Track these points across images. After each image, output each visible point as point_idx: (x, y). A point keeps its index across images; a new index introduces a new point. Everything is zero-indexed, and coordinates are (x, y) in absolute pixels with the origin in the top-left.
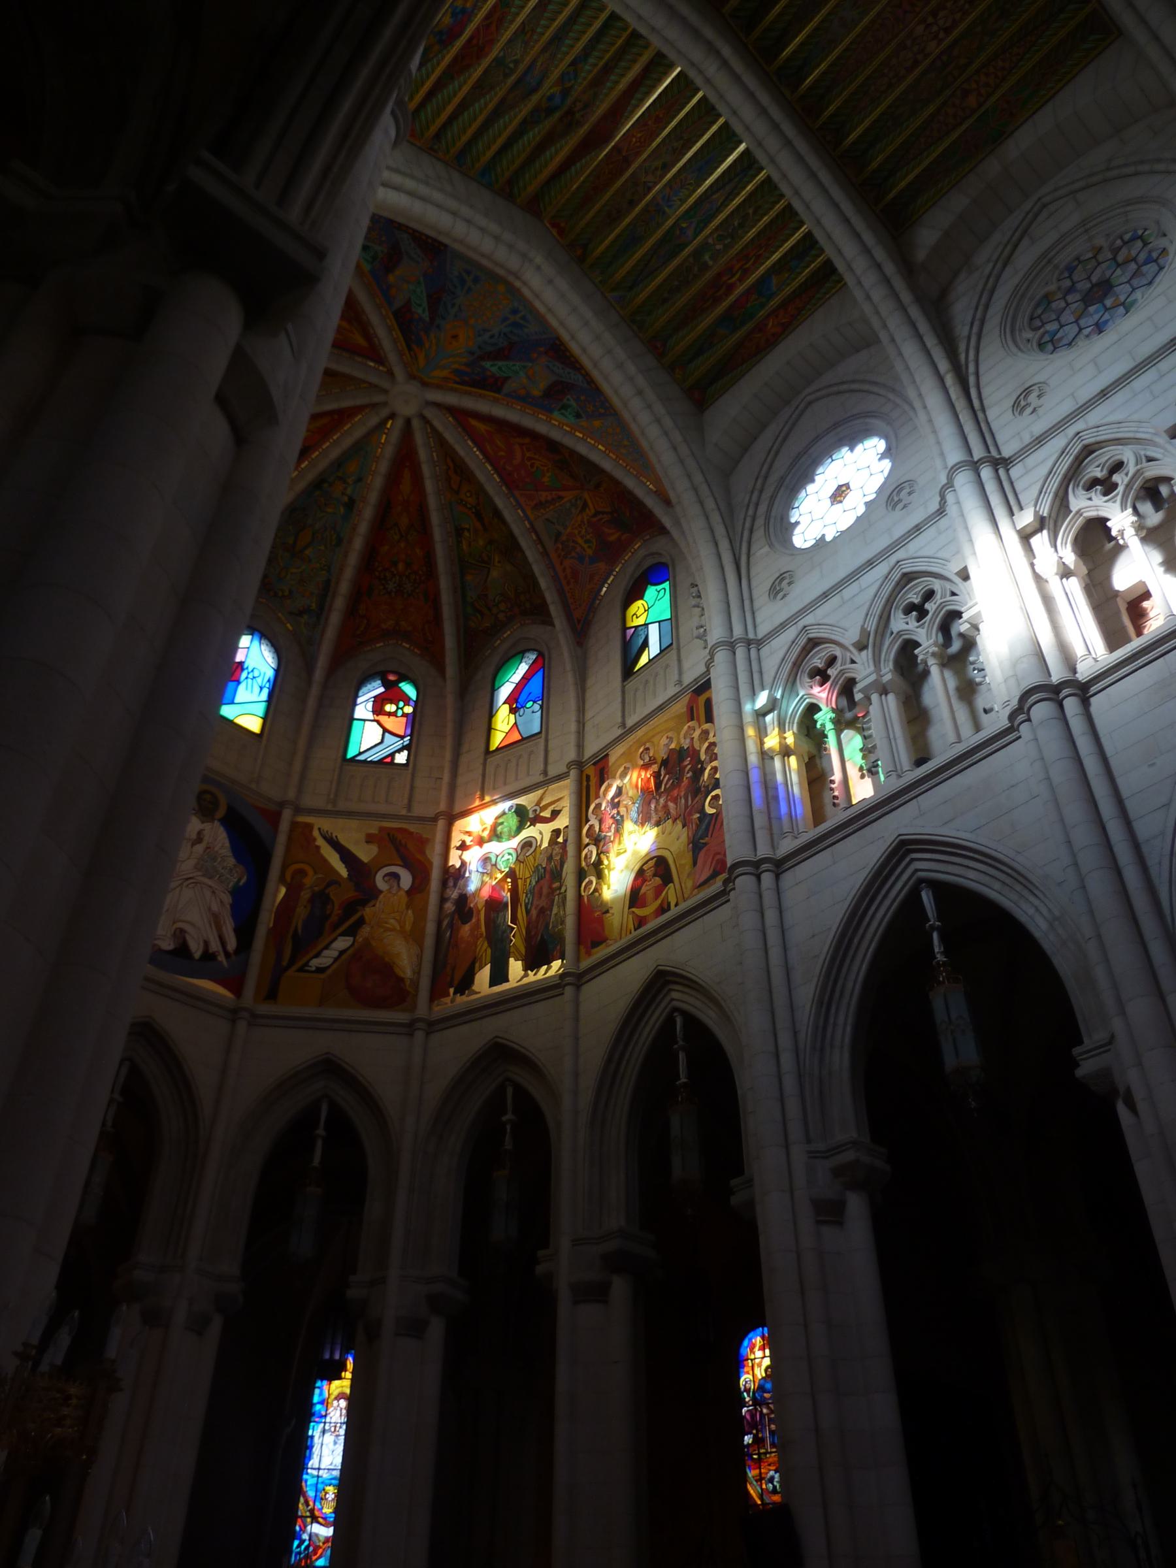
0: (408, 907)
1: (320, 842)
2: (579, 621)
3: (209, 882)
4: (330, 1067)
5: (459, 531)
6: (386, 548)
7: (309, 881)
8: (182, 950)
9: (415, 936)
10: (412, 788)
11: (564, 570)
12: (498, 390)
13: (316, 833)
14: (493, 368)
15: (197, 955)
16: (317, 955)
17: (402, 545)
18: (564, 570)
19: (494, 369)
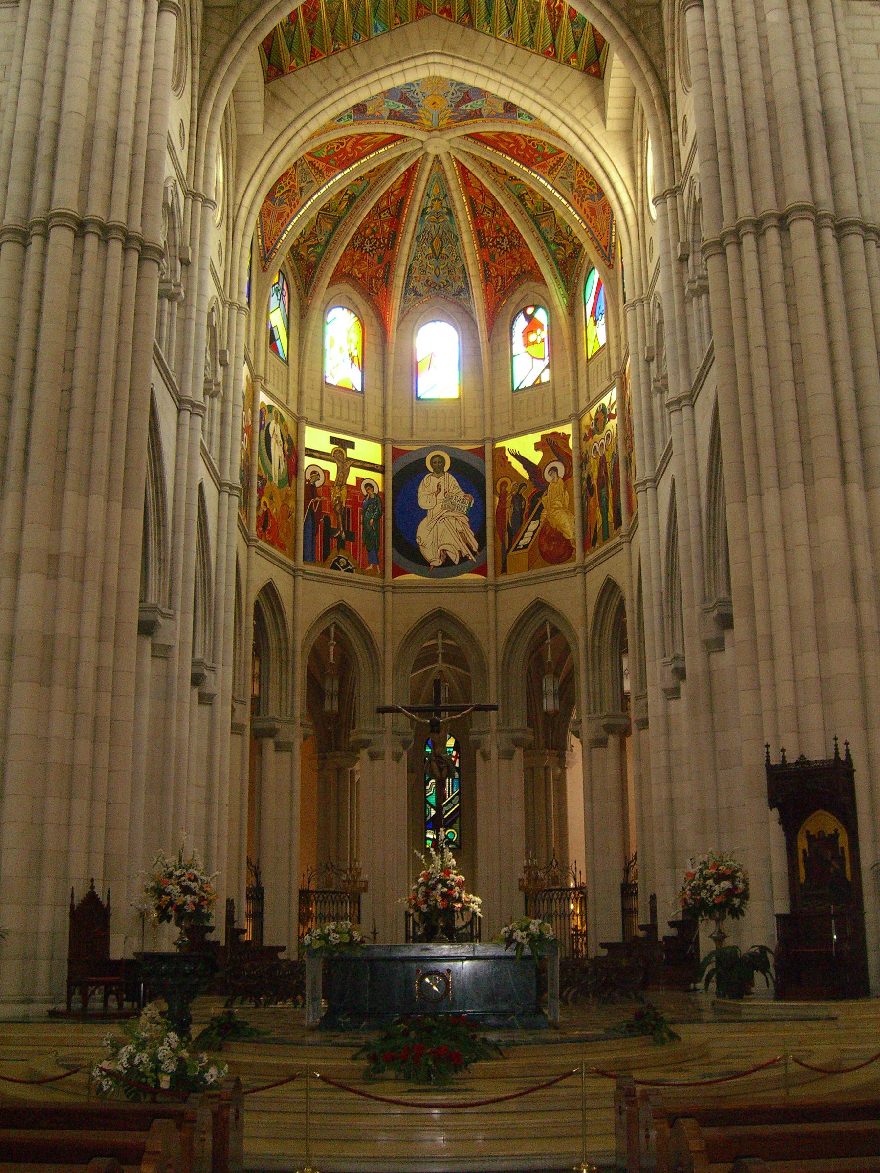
0: (565, 489)
1: (511, 459)
2: (606, 248)
3: (450, 514)
4: (539, 606)
5: (521, 198)
6: (488, 225)
7: (509, 489)
8: (448, 562)
9: (570, 509)
10: (554, 398)
11: (585, 210)
12: (481, 116)
13: (507, 454)
14: (468, 107)
15: (456, 562)
16: (522, 538)
17: (497, 216)
18: (585, 210)
19: (469, 107)
